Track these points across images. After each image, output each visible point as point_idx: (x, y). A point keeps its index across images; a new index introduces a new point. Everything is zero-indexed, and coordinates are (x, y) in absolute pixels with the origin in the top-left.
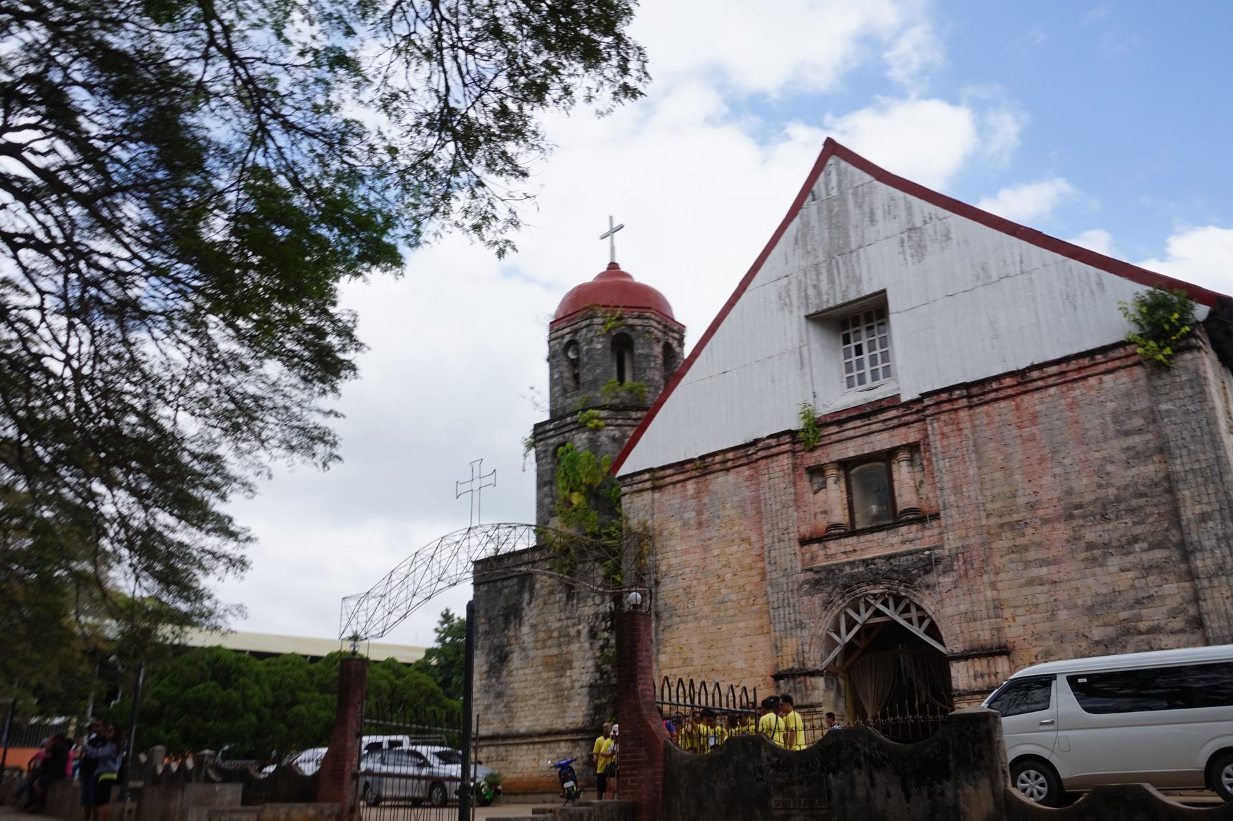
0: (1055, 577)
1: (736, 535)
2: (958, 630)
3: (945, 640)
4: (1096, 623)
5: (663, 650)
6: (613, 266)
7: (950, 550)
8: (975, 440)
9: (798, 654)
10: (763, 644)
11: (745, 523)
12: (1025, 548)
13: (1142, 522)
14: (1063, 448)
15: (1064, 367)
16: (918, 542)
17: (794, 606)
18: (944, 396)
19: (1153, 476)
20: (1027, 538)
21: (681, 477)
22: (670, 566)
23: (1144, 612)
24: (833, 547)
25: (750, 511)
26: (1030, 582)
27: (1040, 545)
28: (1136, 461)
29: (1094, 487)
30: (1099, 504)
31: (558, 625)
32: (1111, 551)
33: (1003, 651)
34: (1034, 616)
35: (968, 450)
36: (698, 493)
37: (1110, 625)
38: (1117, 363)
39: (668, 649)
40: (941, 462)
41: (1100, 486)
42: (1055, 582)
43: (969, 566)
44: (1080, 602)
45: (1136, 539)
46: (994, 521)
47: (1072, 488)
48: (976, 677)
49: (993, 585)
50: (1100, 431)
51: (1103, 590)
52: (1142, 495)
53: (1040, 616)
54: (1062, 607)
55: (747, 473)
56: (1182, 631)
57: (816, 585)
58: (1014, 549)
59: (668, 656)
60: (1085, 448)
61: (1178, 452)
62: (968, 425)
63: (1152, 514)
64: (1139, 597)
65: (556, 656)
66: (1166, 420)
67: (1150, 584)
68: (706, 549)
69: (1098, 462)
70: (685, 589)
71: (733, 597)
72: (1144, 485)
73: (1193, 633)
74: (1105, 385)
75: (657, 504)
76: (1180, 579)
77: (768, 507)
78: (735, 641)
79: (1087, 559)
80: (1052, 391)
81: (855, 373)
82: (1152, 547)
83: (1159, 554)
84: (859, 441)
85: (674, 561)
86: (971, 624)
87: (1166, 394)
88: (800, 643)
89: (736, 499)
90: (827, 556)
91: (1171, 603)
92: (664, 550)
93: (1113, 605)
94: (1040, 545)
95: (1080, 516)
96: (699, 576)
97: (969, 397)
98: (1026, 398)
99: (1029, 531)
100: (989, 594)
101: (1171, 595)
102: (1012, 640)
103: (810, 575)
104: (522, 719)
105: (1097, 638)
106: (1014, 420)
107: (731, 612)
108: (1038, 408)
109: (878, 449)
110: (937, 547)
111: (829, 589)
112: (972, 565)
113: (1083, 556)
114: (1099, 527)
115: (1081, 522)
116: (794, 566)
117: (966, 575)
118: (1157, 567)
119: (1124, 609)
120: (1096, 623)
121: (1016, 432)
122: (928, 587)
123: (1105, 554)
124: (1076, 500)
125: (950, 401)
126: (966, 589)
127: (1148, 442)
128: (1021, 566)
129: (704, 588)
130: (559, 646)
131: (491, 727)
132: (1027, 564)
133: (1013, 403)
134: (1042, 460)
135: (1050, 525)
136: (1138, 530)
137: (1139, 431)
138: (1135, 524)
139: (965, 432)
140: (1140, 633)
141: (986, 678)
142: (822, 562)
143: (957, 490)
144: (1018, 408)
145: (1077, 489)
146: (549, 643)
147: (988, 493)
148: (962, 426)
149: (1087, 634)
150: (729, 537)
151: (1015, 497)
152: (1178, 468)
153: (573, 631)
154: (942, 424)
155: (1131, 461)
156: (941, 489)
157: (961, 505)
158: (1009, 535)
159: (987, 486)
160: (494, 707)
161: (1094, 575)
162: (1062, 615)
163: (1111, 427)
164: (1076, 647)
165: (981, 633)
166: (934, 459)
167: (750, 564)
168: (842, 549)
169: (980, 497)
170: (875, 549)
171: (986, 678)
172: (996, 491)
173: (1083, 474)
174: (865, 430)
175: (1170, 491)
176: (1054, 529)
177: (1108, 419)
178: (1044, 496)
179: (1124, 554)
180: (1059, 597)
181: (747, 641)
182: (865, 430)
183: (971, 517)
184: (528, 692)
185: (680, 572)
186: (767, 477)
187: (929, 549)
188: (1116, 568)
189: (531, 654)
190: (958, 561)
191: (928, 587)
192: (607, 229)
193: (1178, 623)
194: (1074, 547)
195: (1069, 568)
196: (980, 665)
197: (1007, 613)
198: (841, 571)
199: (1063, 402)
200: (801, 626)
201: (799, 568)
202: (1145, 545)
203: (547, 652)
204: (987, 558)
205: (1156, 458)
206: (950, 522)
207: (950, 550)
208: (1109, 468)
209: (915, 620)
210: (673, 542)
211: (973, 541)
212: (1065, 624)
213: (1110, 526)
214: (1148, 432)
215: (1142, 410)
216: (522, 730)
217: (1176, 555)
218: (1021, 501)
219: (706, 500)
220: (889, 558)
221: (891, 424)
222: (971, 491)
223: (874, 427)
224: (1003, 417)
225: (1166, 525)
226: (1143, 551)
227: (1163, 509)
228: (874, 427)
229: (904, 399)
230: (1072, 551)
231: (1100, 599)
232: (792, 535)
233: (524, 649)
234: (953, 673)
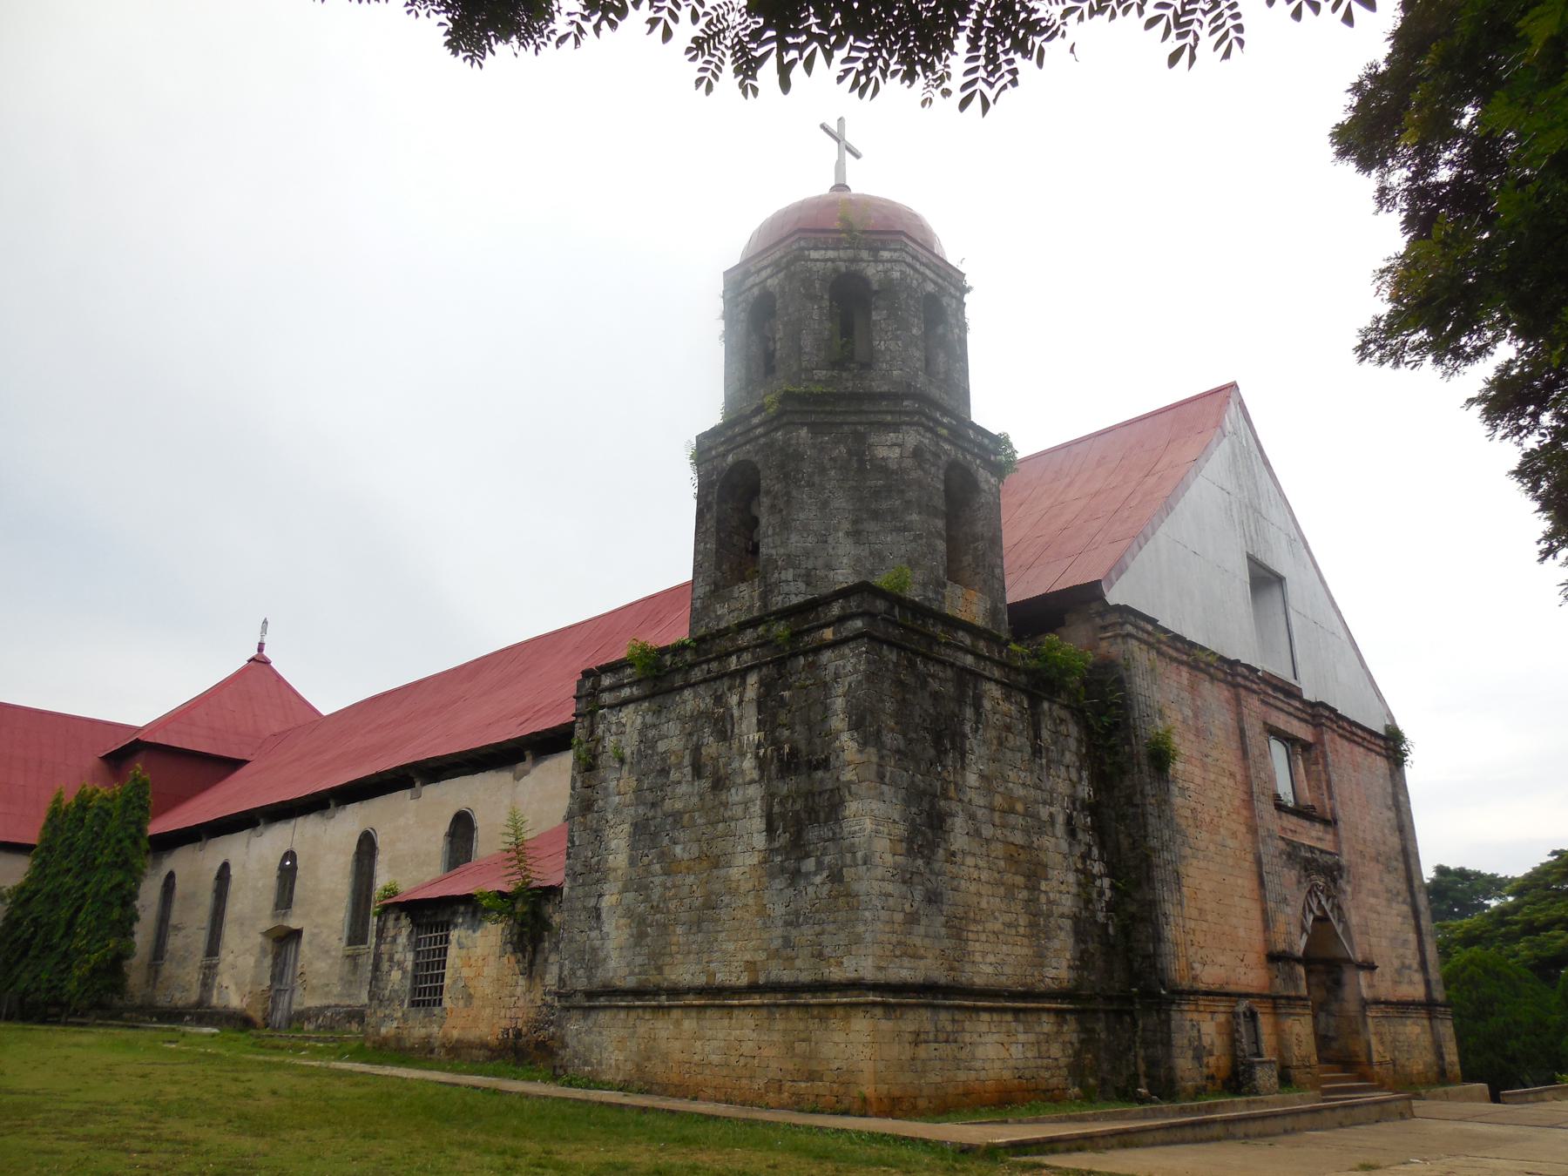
31: (1021, 792)
104: (978, 958)
130: (1027, 831)
131: (922, 963)
153: (1044, 812)
160: (924, 921)
184: (984, 905)
216: (979, 981)
233: (972, 817)
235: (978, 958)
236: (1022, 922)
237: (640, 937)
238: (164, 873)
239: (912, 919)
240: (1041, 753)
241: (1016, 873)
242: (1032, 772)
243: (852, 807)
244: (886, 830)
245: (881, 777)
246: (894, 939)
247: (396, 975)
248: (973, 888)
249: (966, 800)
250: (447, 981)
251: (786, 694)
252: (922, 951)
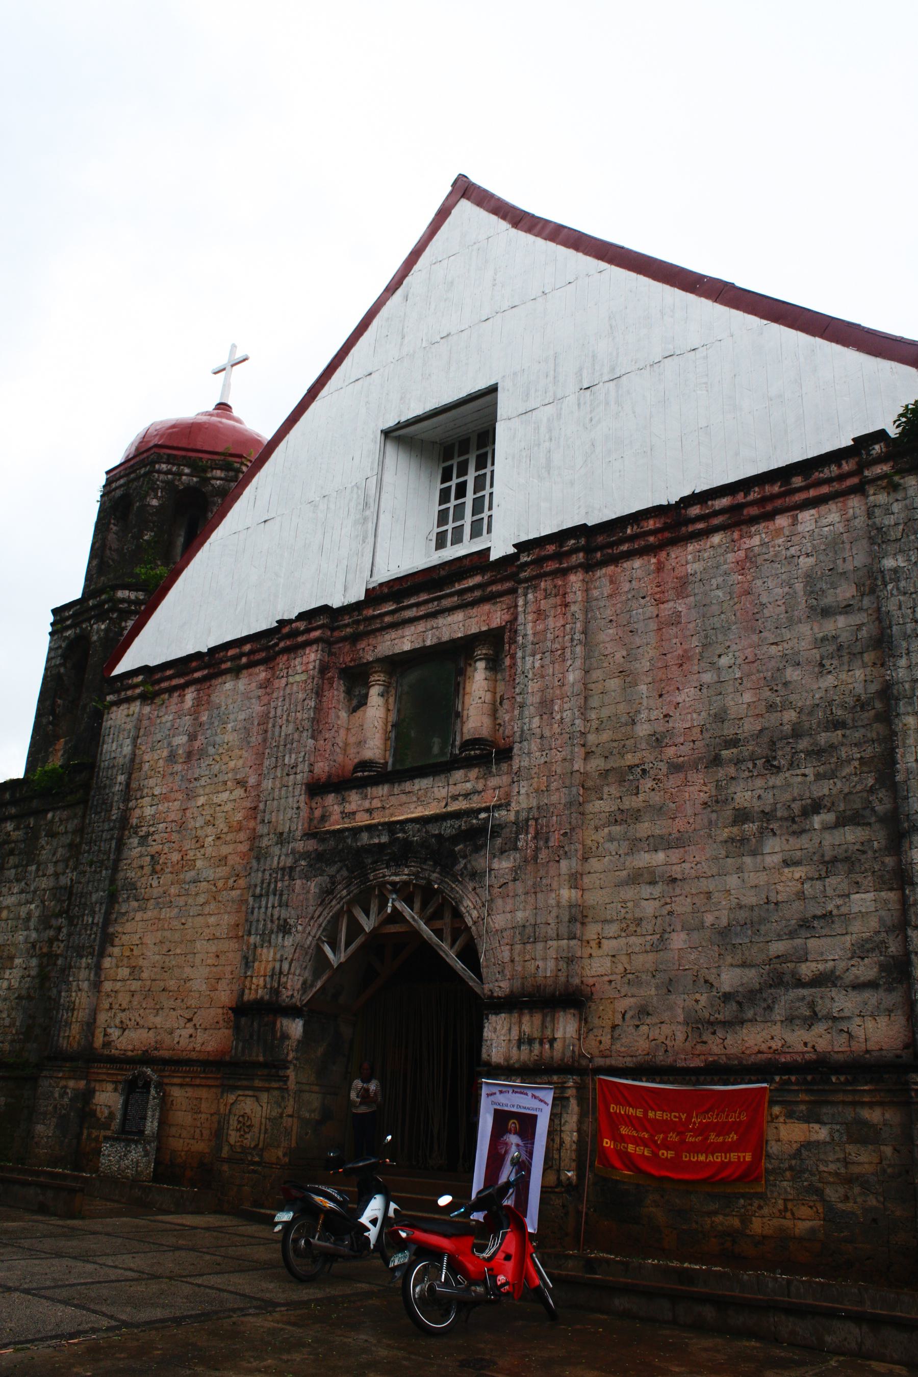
0: (676, 871)
1: (230, 775)
2: (506, 955)
3: (484, 971)
4: (729, 960)
5: (110, 949)
6: (223, 407)
7: (517, 812)
8: (587, 622)
9: (272, 976)
10: (232, 952)
11: (245, 754)
12: (636, 815)
13: (832, 775)
14: (721, 637)
15: (740, 498)
16: (475, 798)
17: (281, 895)
18: (551, 549)
19: (859, 689)
20: (641, 797)
21: (182, 681)
22: (141, 818)
23: (812, 943)
24: (355, 801)
25: (255, 739)
26: (636, 878)
27: (659, 810)
28: (835, 662)
29: (761, 708)
30: (765, 739)
32: (774, 826)
34: (633, 940)
35: (572, 640)
37: (751, 966)
38: (825, 490)
39: (116, 951)
40: (529, 660)
41: (771, 707)
42: (674, 880)
43: (541, 843)
44: (709, 919)
45: (816, 807)
46: (597, 764)
47: (724, 710)
48: (520, 1042)
49: (575, 881)
50: (783, 608)
51: (751, 899)
52: (838, 725)
53: (640, 940)
54: (679, 928)
55: (263, 675)
56: (871, 985)
57: (318, 861)
58: (621, 817)
59: (114, 960)
60: (755, 638)
61: (904, 644)
62: (579, 596)
63: (849, 761)
64: (809, 915)
66: (890, 587)
67: (829, 892)
68: (190, 795)
69: (773, 664)
70: (152, 857)
72: (843, 706)
73: (890, 990)
74: (800, 528)
75: (145, 723)
76: (882, 884)
77: (277, 729)
78: (198, 944)
79: (731, 840)
80: (716, 539)
81: (450, 527)
82: (841, 822)
83: (851, 835)
84: (421, 626)
85: (149, 811)
86: (529, 947)
87: (897, 540)
88: (278, 956)
89: (242, 716)
90: (345, 815)
91: (860, 929)
92: (139, 794)
93: (763, 929)
94: (659, 810)
95: (731, 760)
96: (175, 837)
97: (588, 550)
98: (675, 552)
99: (647, 784)
100: (566, 894)
101: (863, 915)
102: (591, 981)
103: (311, 845)
105: (726, 988)
106: (651, 589)
108: (690, 569)
109: (445, 638)
110: (498, 807)
111: (332, 870)
112: (547, 840)
113: (725, 833)
114: (759, 782)
115: (732, 771)
116: (294, 827)
117: (535, 858)
118: (847, 859)
119: (780, 938)
120: (729, 960)
121: (651, 610)
123: (761, 831)
124: (729, 730)
125: (558, 556)
126: (530, 883)
127: (859, 627)
128: (624, 847)
129: (175, 857)
132: (635, 845)
133: (653, 560)
134: (683, 660)
135: (682, 775)
136: (823, 789)
137: (847, 609)
138: (819, 777)
139: (574, 608)
140: (800, 983)
141: (537, 1046)
142: (335, 824)
143: (546, 707)
144: (660, 568)
145: (733, 713)
147: (593, 715)
148: (570, 598)
149: (712, 978)
150: (222, 778)
151: (634, 723)
152: (902, 673)
154: (540, 594)
155: (827, 662)
156: (522, 706)
157: (547, 733)
158: (614, 790)
159: (595, 702)
161: (740, 869)
162: (678, 940)
163: (801, 599)
164: (690, 1003)
165: (540, 963)
166: (519, 654)
167: (239, 822)
168: (366, 804)
169: (577, 722)
170: (412, 806)
171: (537, 1046)
172: (605, 713)
173: (747, 684)
174: (432, 607)
175: (887, 717)
176: (686, 783)
177: (799, 587)
178: (679, 724)
179: (794, 833)
180: (678, 909)
181: (213, 948)
182: (432, 607)
183: (559, 756)
186: (284, 681)
187: (486, 809)
188: (777, 859)
190: (527, 833)
192: (223, 361)
193: (866, 970)
194: (714, 816)
196: (530, 1024)
197: (592, 931)
199: (730, 557)
201: (299, 834)
202: (830, 817)
204: (572, 829)
205: (869, 657)
206: (525, 763)
207: (517, 812)
208: (792, 674)
209: (447, 933)
210: (152, 782)
211: (554, 798)
212: (680, 958)
213: (777, 780)
214: (860, 609)
215: (856, 569)
217: (878, 837)
218: (643, 730)
219: (204, 718)
221: (469, 597)
222: (566, 711)
223: (446, 603)
224: (635, 584)
225: (871, 782)
226: (826, 828)
227: (869, 751)
228: (446, 603)
229: (493, 556)
230: (710, 822)
231: (742, 915)
232: (299, 777)
234: (487, 1033)
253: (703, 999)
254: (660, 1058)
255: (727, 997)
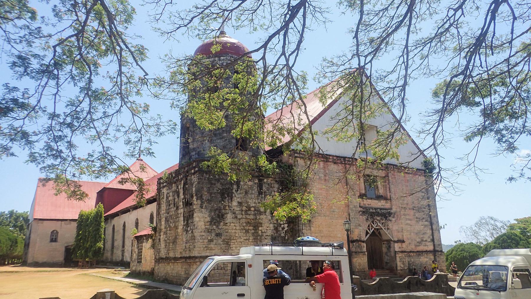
0: (411, 224)
26: (407, 224)
31: (254, 205)
33: (403, 242)
36: (324, 168)
39: (314, 225)
51: (419, 230)
65: (253, 219)
71: (337, 210)
80: (411, 175)
90: (364, 204)
103: (362, 209)
104: (234, 248)
107: (336, 216)
111: (367, 215)
122: (390, 220)
130: (255, 215)
146: (249, 212)
160: (214, 241)
168: (367, 203)
184: (237, 235)
185: (318, 196)
189: (239, 216)
191: (390, 220)
195: (413, 222)
198: (370, 210)
200: (360, 225)
203: (248, 217)
220: (381, 209)
233: (234, 213)
235: (234, 248)
236: (251, 238)
237: (166, 245)
238: (113, 225)
239: (211, 241)
240: (262, 193)
241: (250, 226)
242: (258, 199)
243: (195, 215)
244: (203, 220)
245: (202, 207)
246: (204, 246)
247: (135, 255)
248: (233, 231)
249: (232, 209)
250: (143, 256)
251: (187, 186)
252: (214, 248)
253: (416, 242)
254: (412, 250)
255: (418, 242)
